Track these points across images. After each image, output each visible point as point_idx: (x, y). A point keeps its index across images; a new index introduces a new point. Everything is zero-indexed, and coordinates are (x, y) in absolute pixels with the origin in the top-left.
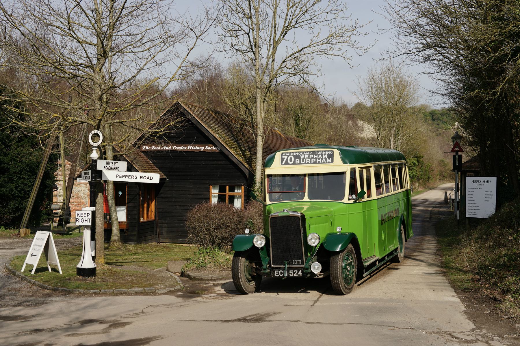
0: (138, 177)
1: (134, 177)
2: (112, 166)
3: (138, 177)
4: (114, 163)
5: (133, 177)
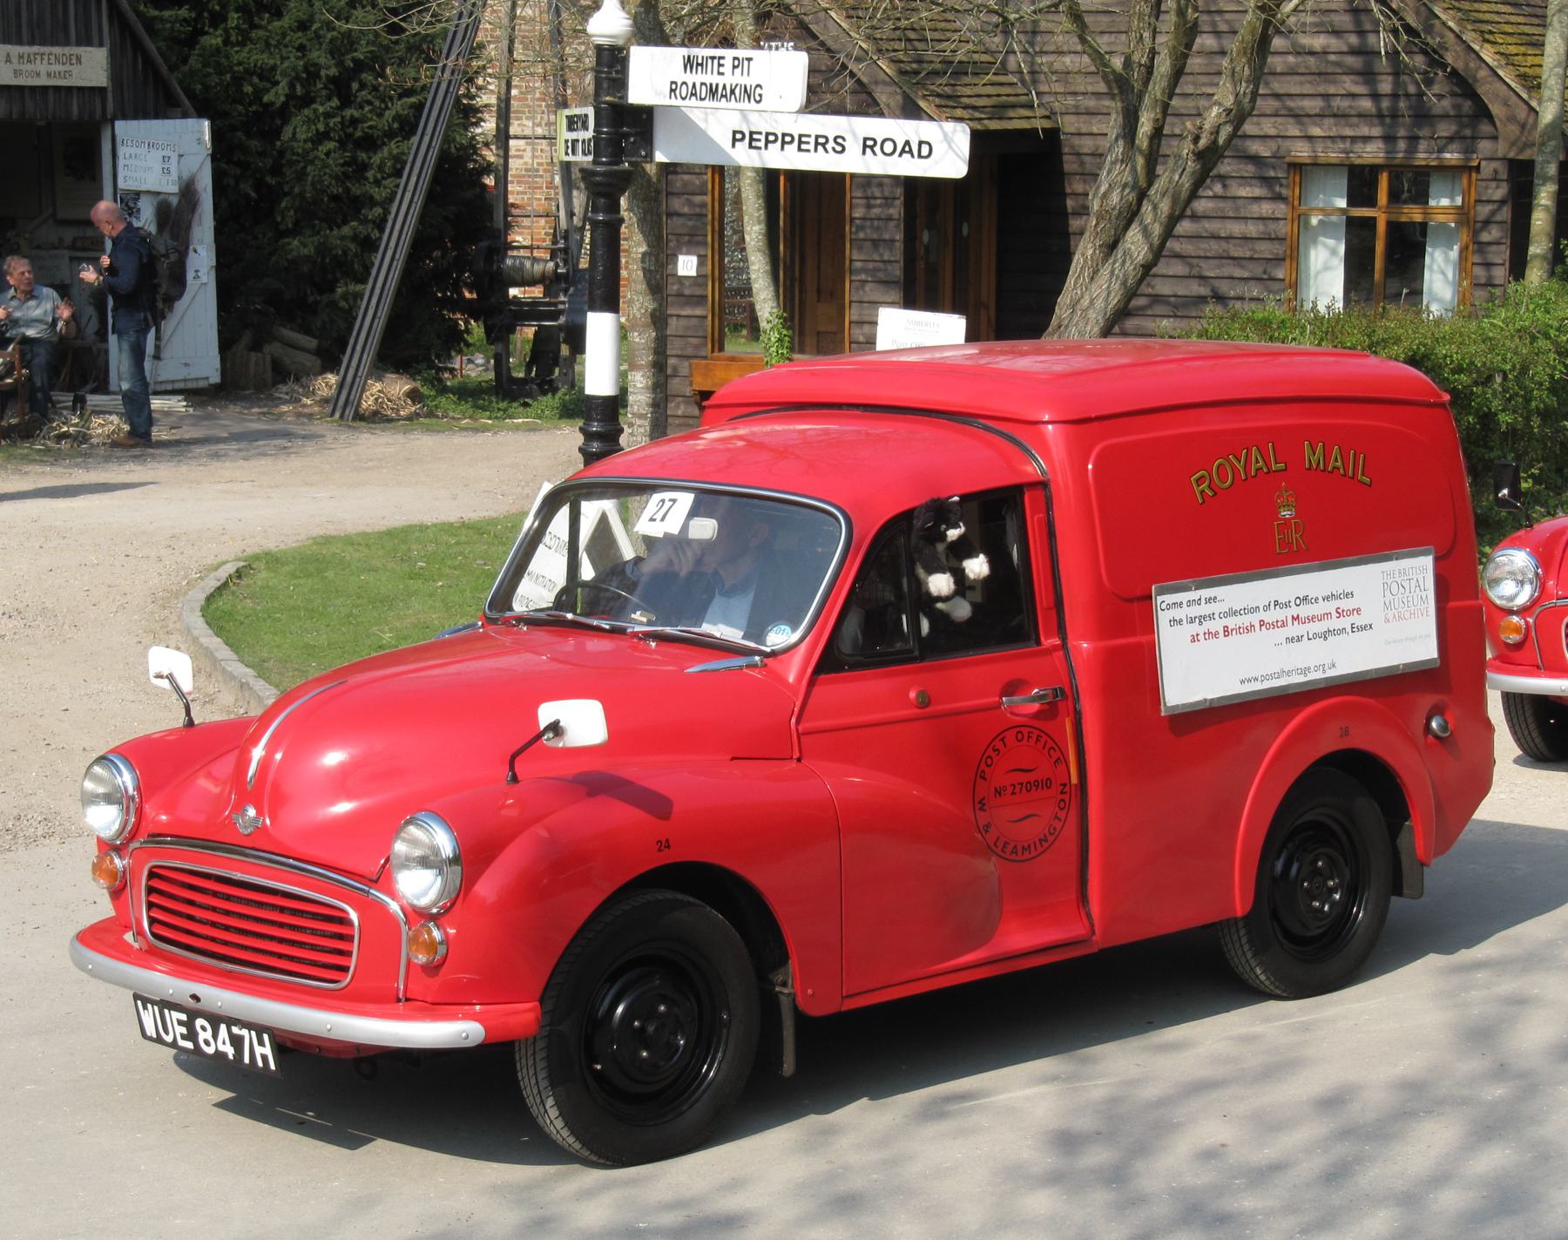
0: (853, 147)
1: (831, 145)
2: (721, 80)
3: (853, 147)
4: (728, 63)
5: (821, 142)
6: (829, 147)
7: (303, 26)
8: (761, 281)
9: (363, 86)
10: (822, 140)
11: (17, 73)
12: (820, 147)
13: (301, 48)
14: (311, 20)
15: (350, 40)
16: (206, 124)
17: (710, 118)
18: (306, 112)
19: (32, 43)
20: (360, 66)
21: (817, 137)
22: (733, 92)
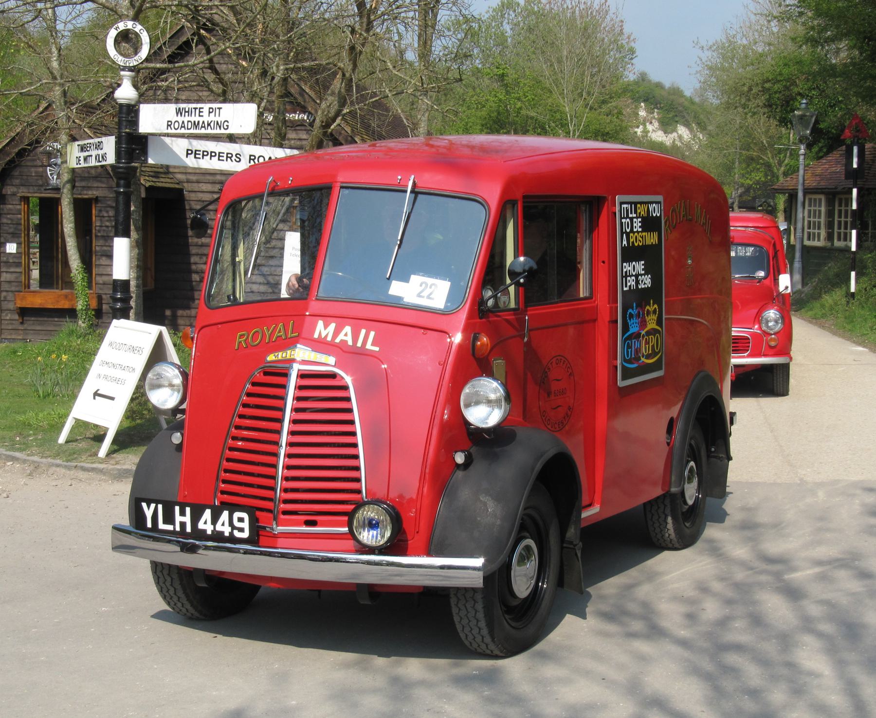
1: (234, 158)
2: (201, 120)
5: (229, 156)
6: (233, 159)
8: (72, 251)
10: (229, 155)
12: (229, 159)
17: (174, 143)
21: (227, 154)
22: (209, 125)
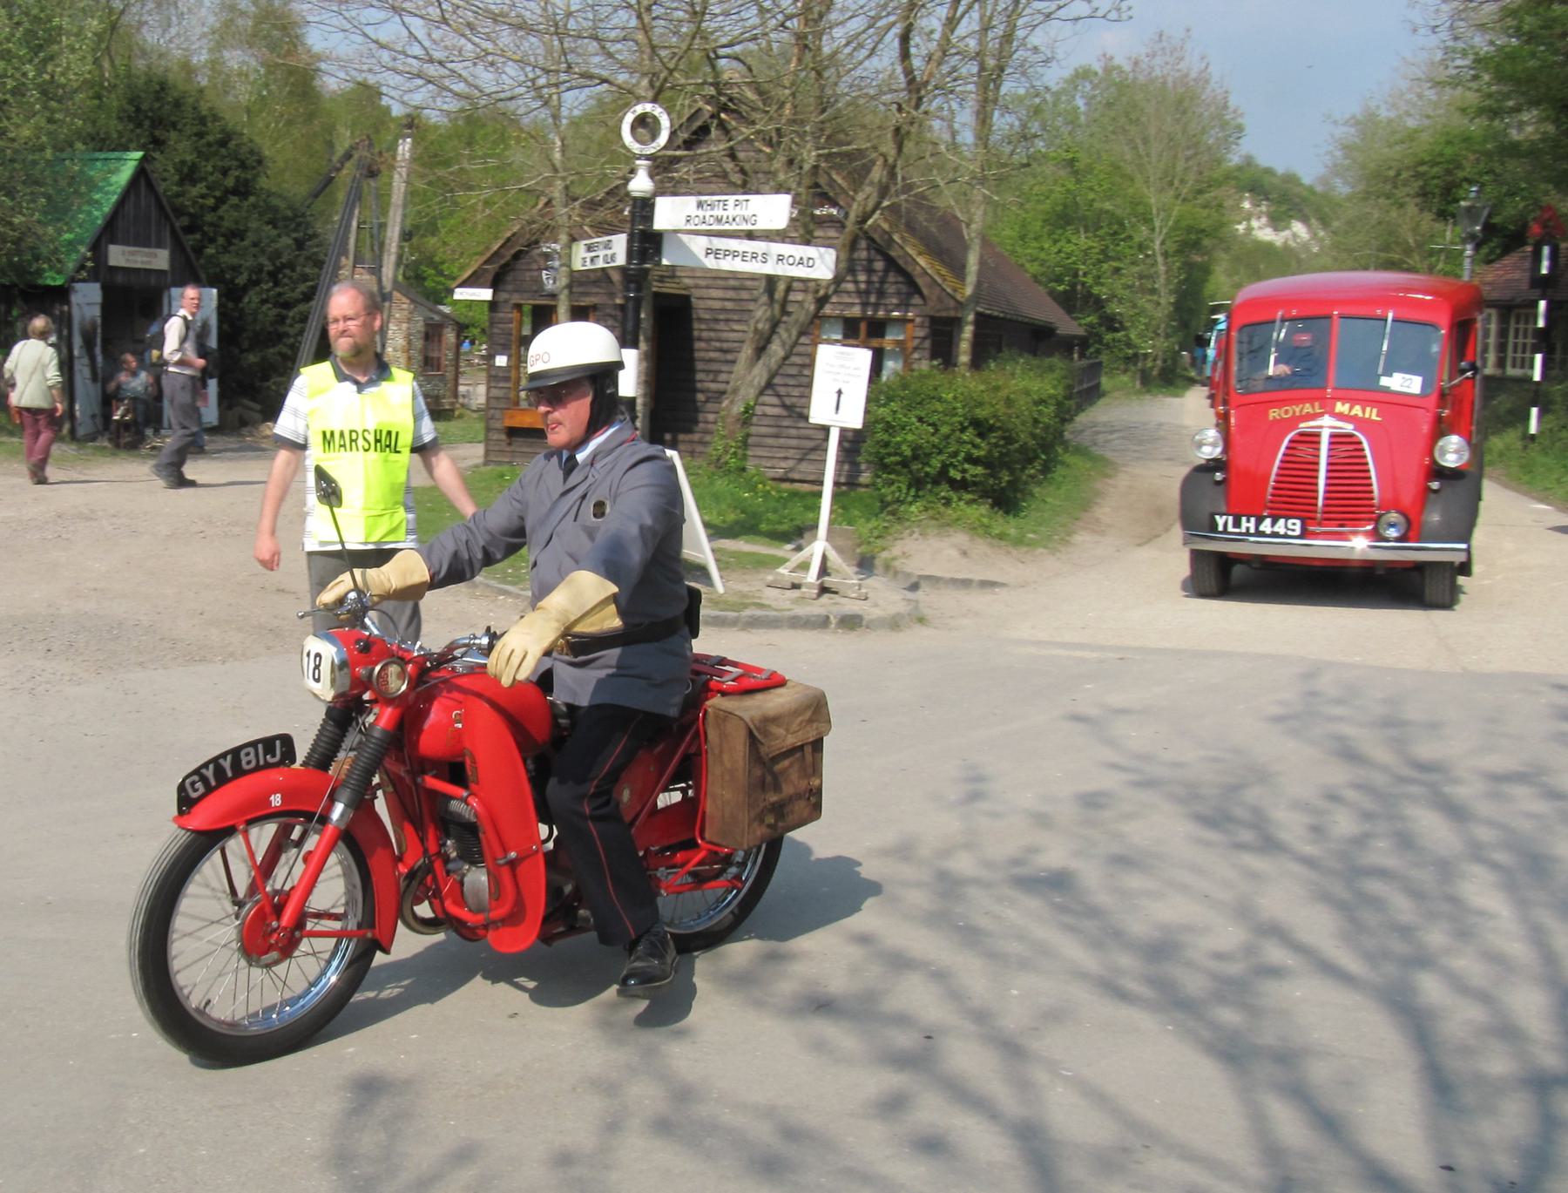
0: (772, 260)
1: (760, 258)
2: (725, 214)
3: (772, 260)
5: (754, 256)
7: (255, 245)
9: (285, 276)
11: (128, 260)
13: (254, 256)
14: (260, 242)
15: (278, 254)
16: (215, 291)
18: (258, 288)
19: (135, 245)
20: (284, 266)
